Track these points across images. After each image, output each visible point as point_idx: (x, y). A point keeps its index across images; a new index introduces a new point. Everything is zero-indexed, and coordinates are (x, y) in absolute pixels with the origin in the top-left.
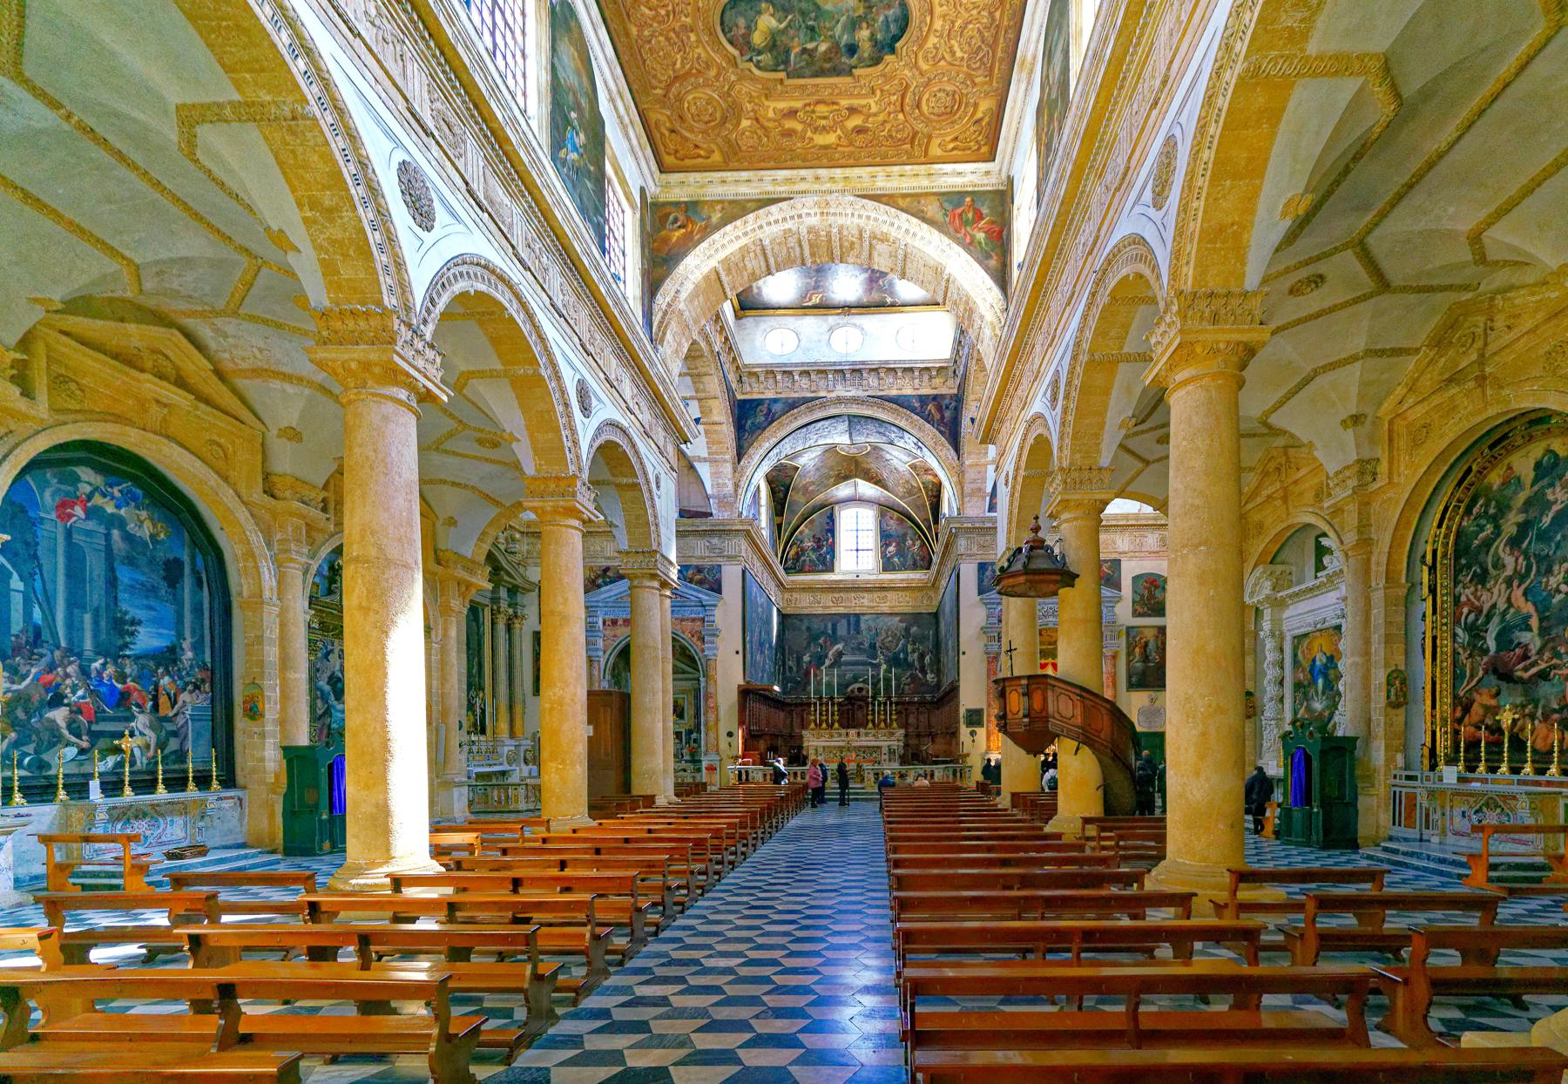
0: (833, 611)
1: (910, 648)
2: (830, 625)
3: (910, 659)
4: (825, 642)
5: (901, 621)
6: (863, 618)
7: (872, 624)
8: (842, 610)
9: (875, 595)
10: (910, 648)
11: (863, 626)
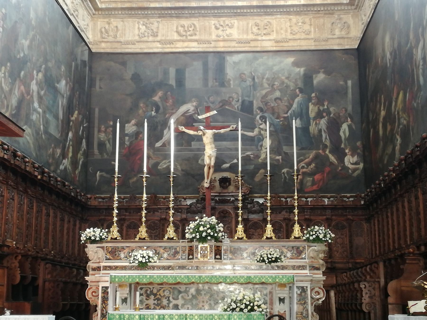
0: (180, 47)
1: (313, 110)
2: (172, 72)
3: (313, 128)
4: (164, 99)
5: (296, 64)
6: (230, 60)
7: (246, 69)
8: (194, 47)
9: (251, 21)
10: (313, 110)
11: (230, 72)
